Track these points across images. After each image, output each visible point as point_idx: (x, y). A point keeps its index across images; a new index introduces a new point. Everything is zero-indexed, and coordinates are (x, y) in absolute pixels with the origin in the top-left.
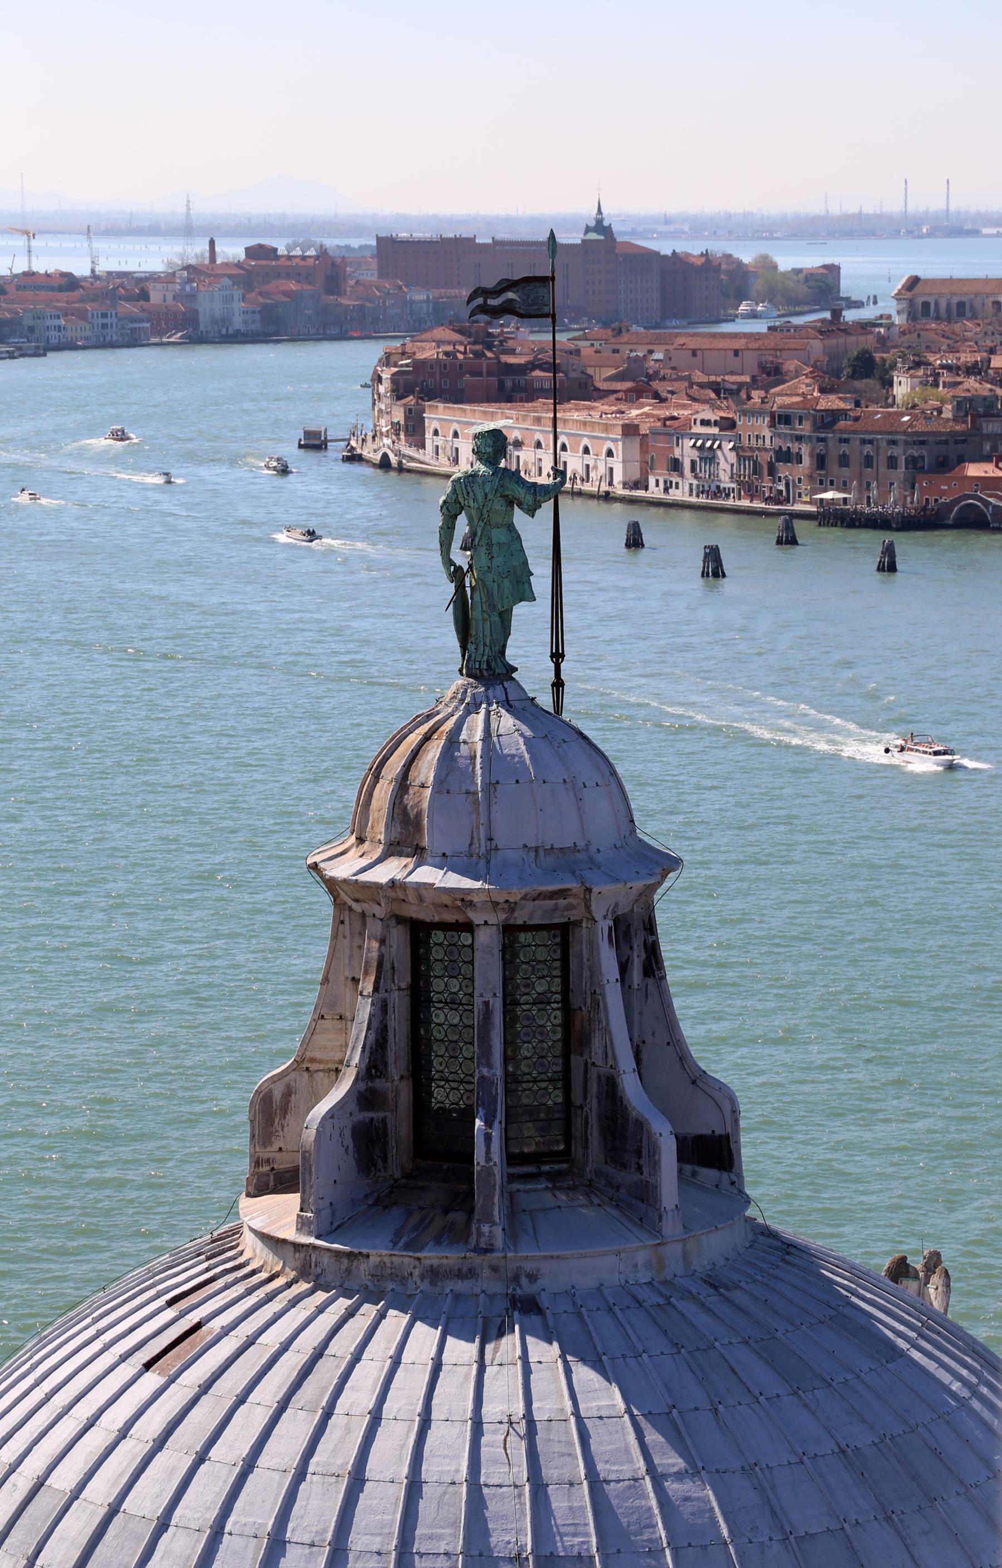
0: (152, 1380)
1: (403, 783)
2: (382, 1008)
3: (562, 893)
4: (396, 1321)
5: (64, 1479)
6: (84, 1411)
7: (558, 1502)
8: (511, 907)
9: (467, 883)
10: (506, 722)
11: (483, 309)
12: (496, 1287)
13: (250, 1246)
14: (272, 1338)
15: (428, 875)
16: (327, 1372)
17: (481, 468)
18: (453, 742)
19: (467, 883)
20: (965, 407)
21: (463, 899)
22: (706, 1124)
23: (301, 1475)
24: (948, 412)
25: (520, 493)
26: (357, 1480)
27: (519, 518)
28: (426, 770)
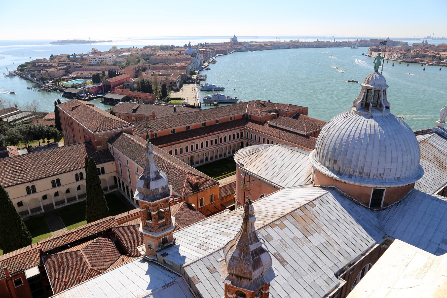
0: (344, 119)
1: (368, 79)
2: (364, 95)
3: (379, 88)
4: (362, 117)
5: (337, 125)
6: (339, 120)
7: (372, 131)
8: (375, 89)
9: (372, 87)
10: (377, 75)
11: (381, 44)
12: (370, 116)
13: (352, 111)
14: (353, 117)
15: (370, 86)
16: (356, 120)
17: (378, 56)
18: (373, 76)
19: (372, 87)
20: (417, 53)
21: (372, 88)
22: (388, 106)
23: (354, 126)
24: (415, 54)
25: (381, 58)
26: (358, 127)
27: (381, 60)
28: (370, 78)
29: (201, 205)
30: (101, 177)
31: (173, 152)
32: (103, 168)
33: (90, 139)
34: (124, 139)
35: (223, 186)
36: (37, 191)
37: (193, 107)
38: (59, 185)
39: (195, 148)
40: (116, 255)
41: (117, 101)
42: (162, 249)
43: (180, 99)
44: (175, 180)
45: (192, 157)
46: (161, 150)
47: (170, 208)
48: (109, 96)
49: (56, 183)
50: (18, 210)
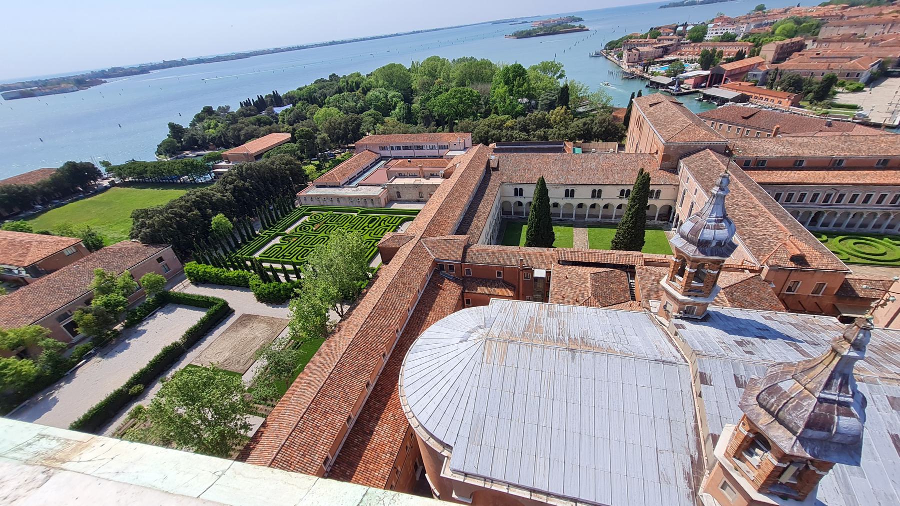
29: (789, 289)
30: (650, 202)
31: (784, 196)
32: (659, 192)
33: (657, 151)
34: (706, 160)
35: (857, 277)
36: (575, 197)
37: (877, 126)
38: (599, 196)
39: (833, 199)
40: (625, 297)
41: (723, 101)
42: (682, 318)
43: (854, 107)
44: (760, 239)
45: (819, 214)
46: (760, 189)
47: (719, 273)
48: (713, 91)
49: (597, 194)
50: (552, 210)
